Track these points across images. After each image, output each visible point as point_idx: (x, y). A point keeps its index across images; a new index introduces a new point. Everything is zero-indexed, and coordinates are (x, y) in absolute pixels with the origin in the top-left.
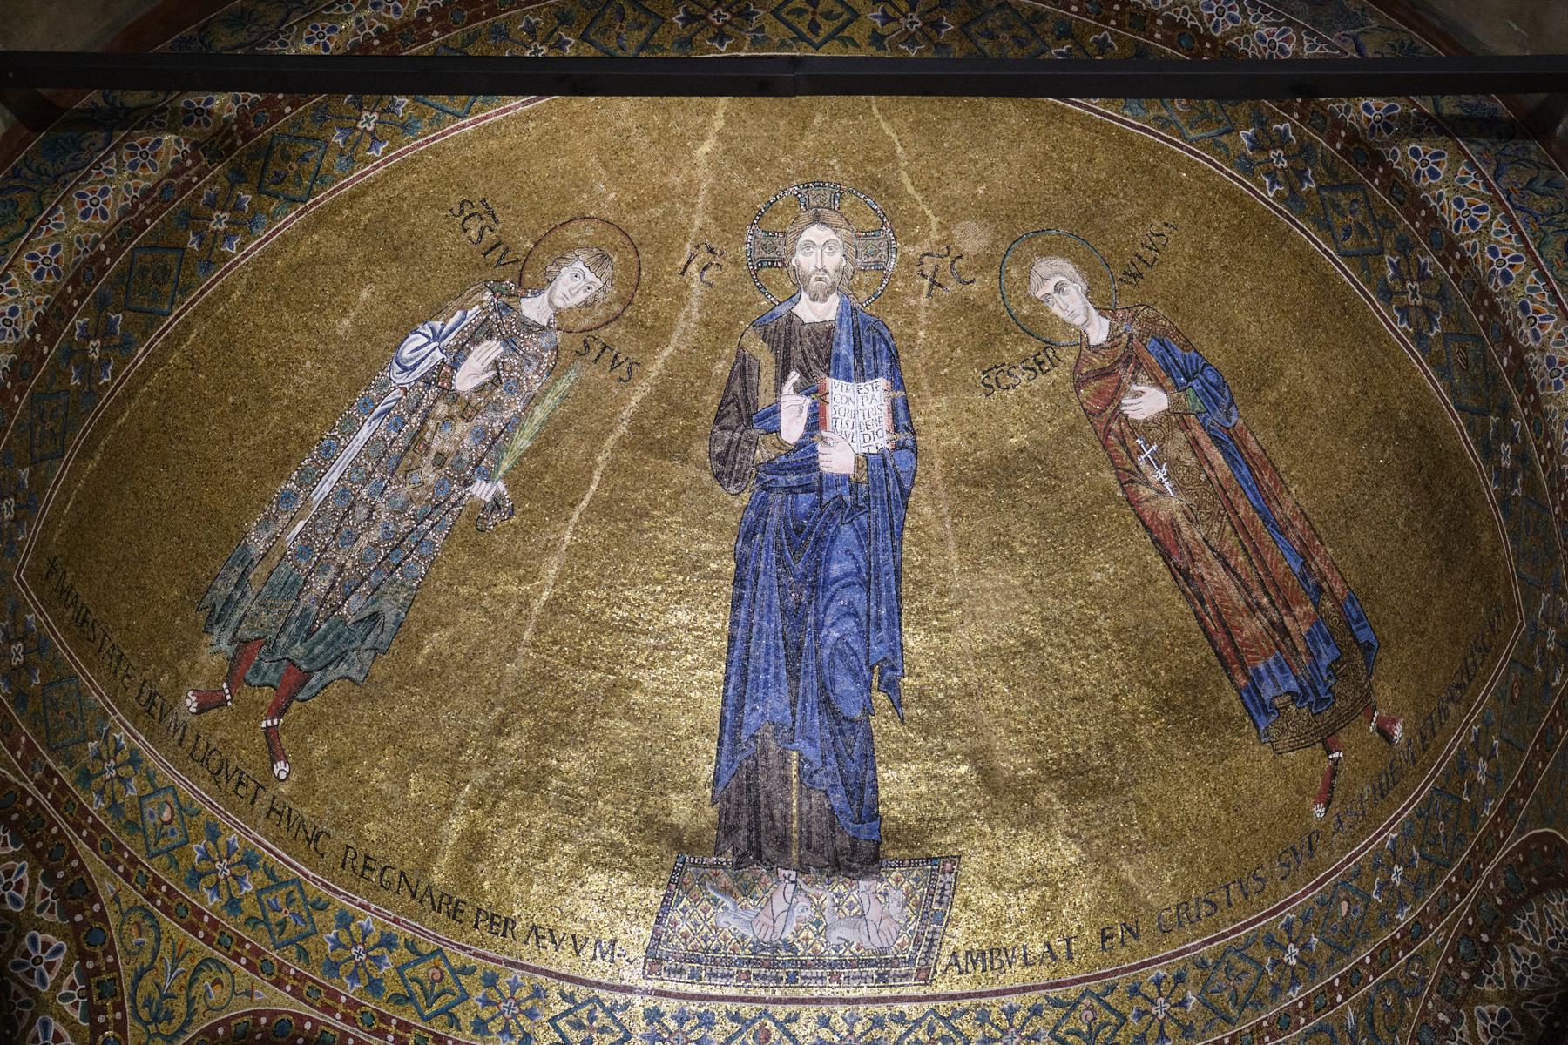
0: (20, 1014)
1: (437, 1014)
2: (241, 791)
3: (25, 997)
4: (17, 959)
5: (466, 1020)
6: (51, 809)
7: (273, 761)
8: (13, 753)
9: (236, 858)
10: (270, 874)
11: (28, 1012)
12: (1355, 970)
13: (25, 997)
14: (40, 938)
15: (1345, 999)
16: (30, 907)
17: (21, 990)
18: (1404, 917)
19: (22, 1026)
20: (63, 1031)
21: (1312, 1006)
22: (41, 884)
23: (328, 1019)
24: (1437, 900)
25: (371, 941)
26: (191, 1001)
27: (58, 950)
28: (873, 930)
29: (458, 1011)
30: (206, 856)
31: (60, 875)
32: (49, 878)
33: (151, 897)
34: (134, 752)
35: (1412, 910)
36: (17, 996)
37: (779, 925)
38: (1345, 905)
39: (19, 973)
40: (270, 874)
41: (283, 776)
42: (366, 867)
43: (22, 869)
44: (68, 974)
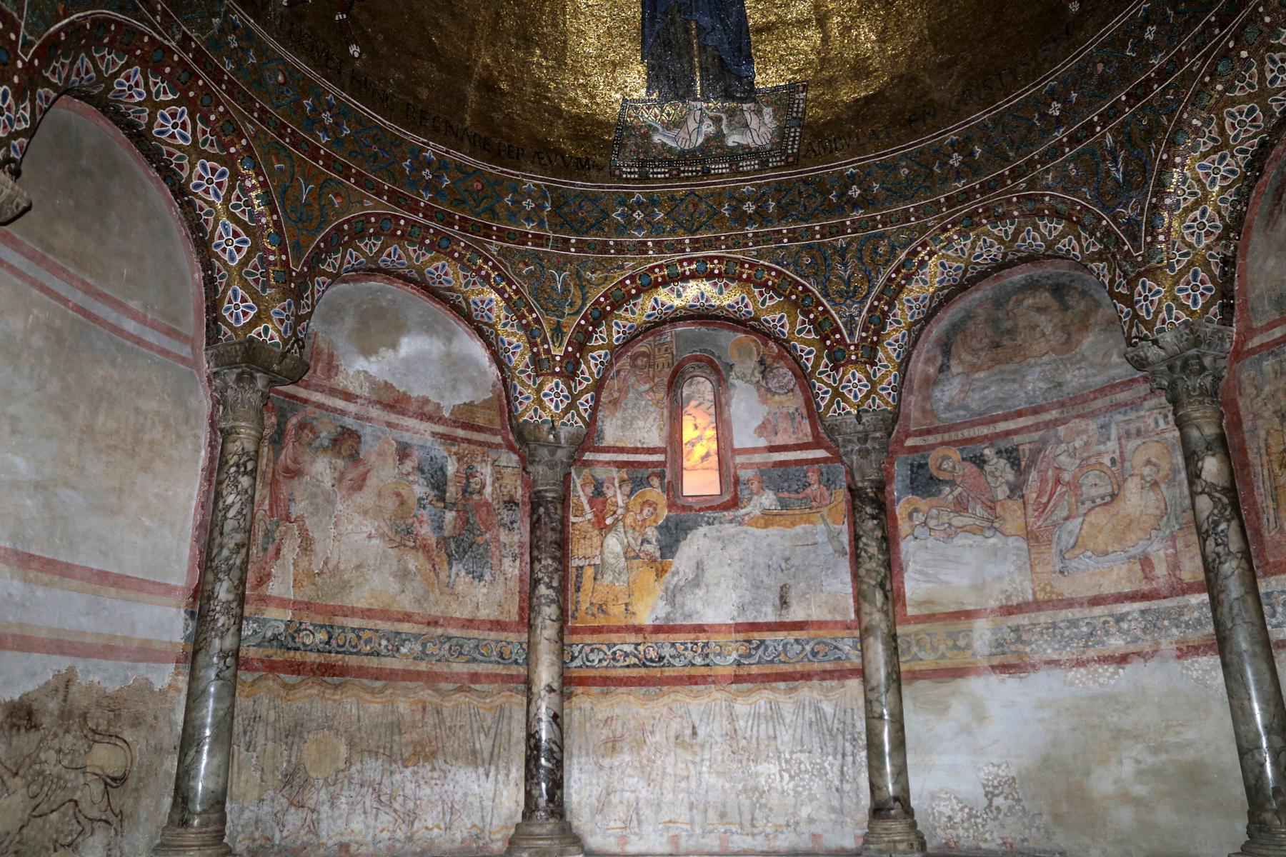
0: (206, 221)
1: (484, 211)
2: (331, 64)
3: (207, 209)
4: (195, 181)
5: (503, 213)
6: (195, 66)
7: (348, 45)
8: (154, 17)
9: (335, 110)
10: (359, 123)
11: (211, 218)
12: (1113, 106)
13: (207, 209)
14: (208, 164)
15: (1103, 128)
16: (195, 141)
17: (203, 204)
18: (1156, 62)
19: (209, 229)
20: (238, 229)
21: (1074, 140)
22: (199, 124)
23: (414, 217)
24: (1194, 39)
25: (435, 166)
26: (322, 208)
27: (223, 174)
28: (755, 134)
29: (497, 208)
30: (314, 109)
31: (213, 118)
32: (206, 120)
33: (282, 136)
34: (247, 29)
35: (1167, 54)
36: (201, 209)
37: (694, 136)
38: (1100, 67)
39: (199, 191)
40: (359, 123)
41: (356, 55)
42: (422, 118)
43: (183, 112)
44: (234, 189)
